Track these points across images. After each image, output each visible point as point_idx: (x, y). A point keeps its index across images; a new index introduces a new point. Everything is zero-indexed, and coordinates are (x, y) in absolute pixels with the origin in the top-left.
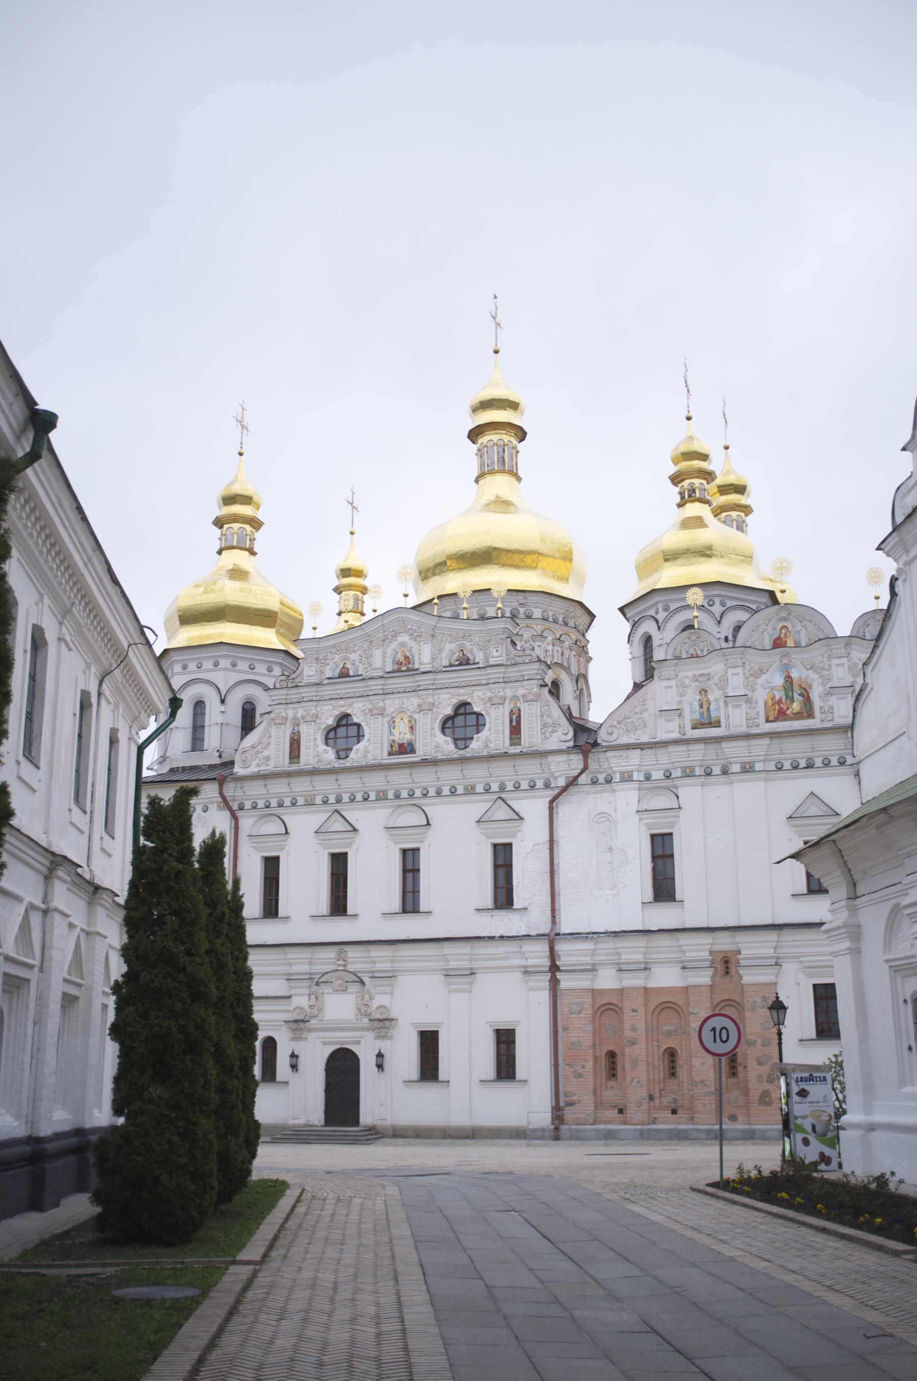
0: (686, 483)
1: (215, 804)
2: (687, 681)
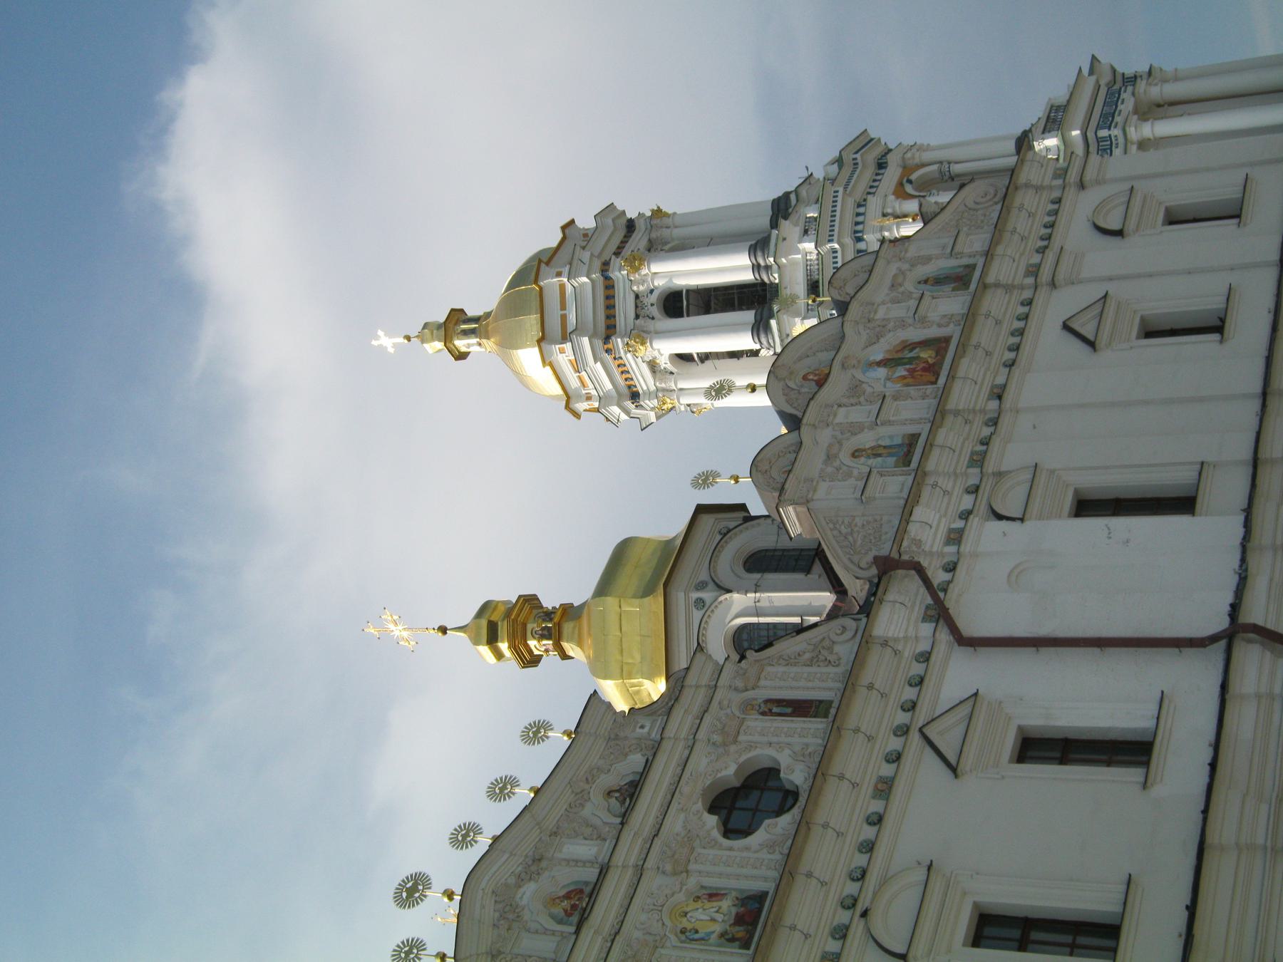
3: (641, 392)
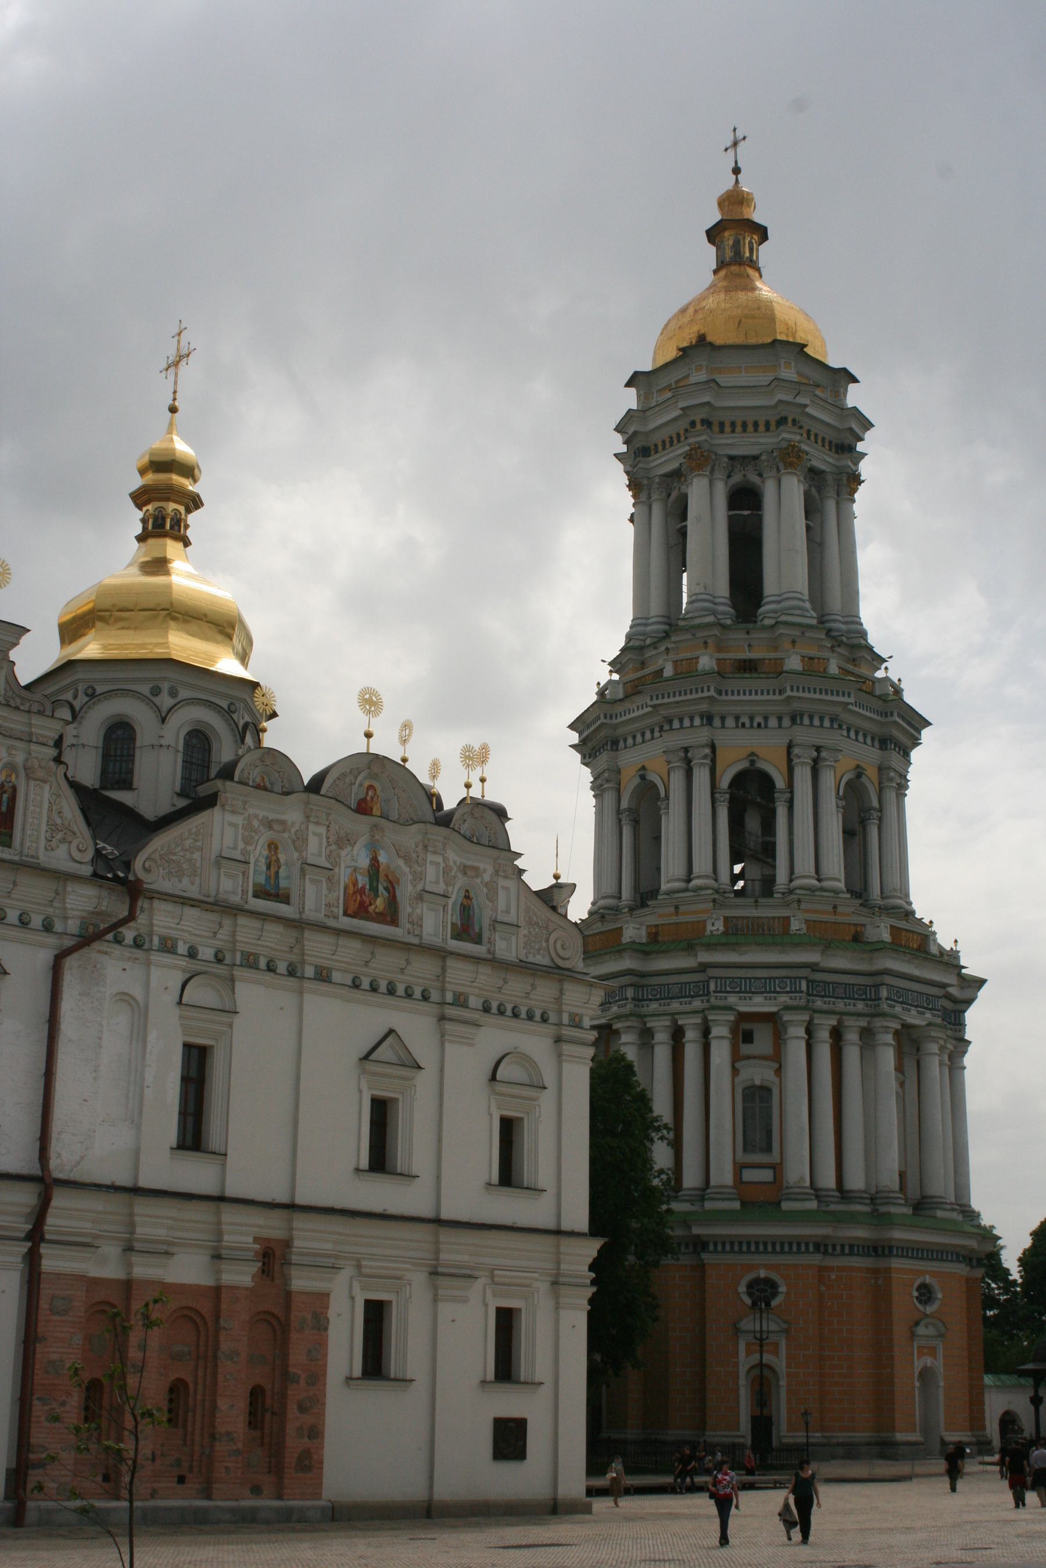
2: (256, 823)
3: (650, 459)
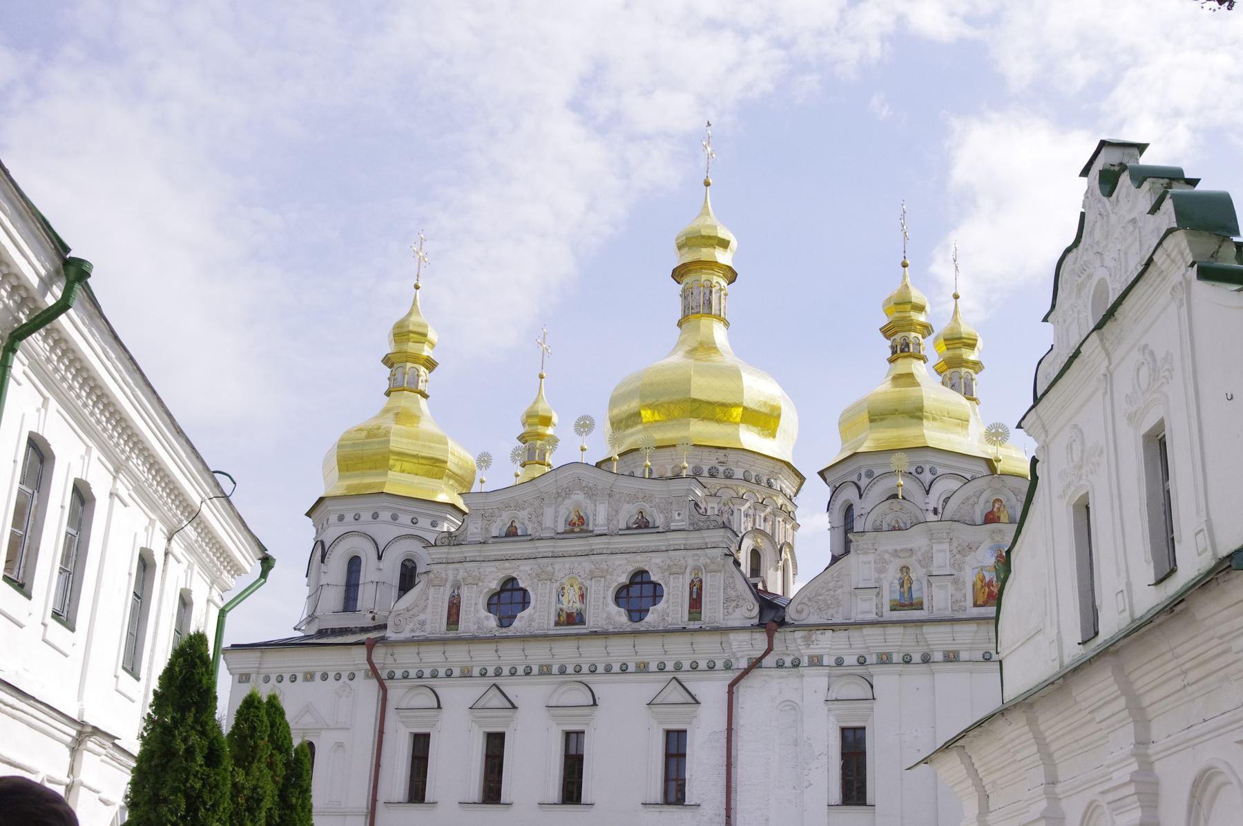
0: (898, 337)
1: (363, 672)
2: (887, 556)
